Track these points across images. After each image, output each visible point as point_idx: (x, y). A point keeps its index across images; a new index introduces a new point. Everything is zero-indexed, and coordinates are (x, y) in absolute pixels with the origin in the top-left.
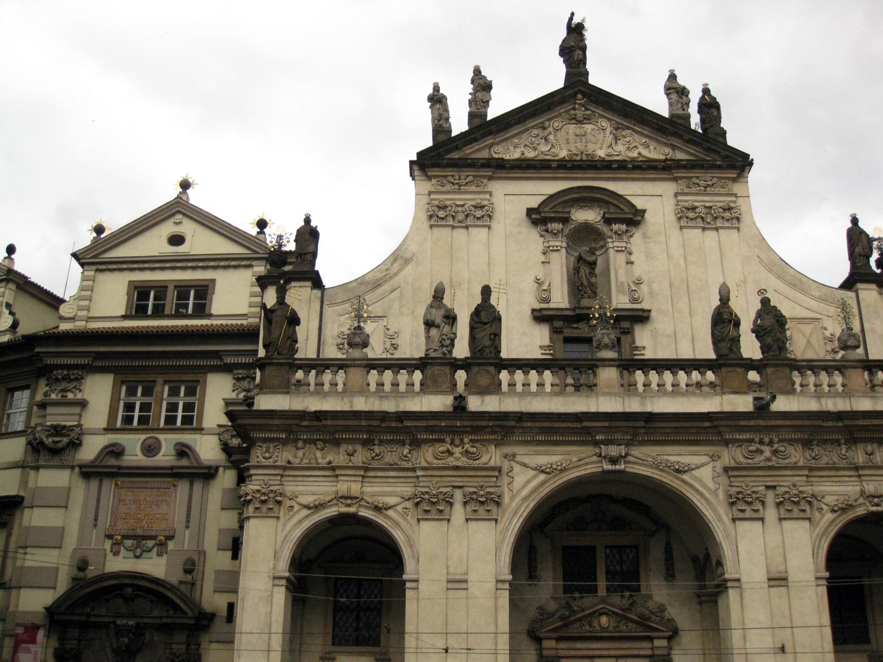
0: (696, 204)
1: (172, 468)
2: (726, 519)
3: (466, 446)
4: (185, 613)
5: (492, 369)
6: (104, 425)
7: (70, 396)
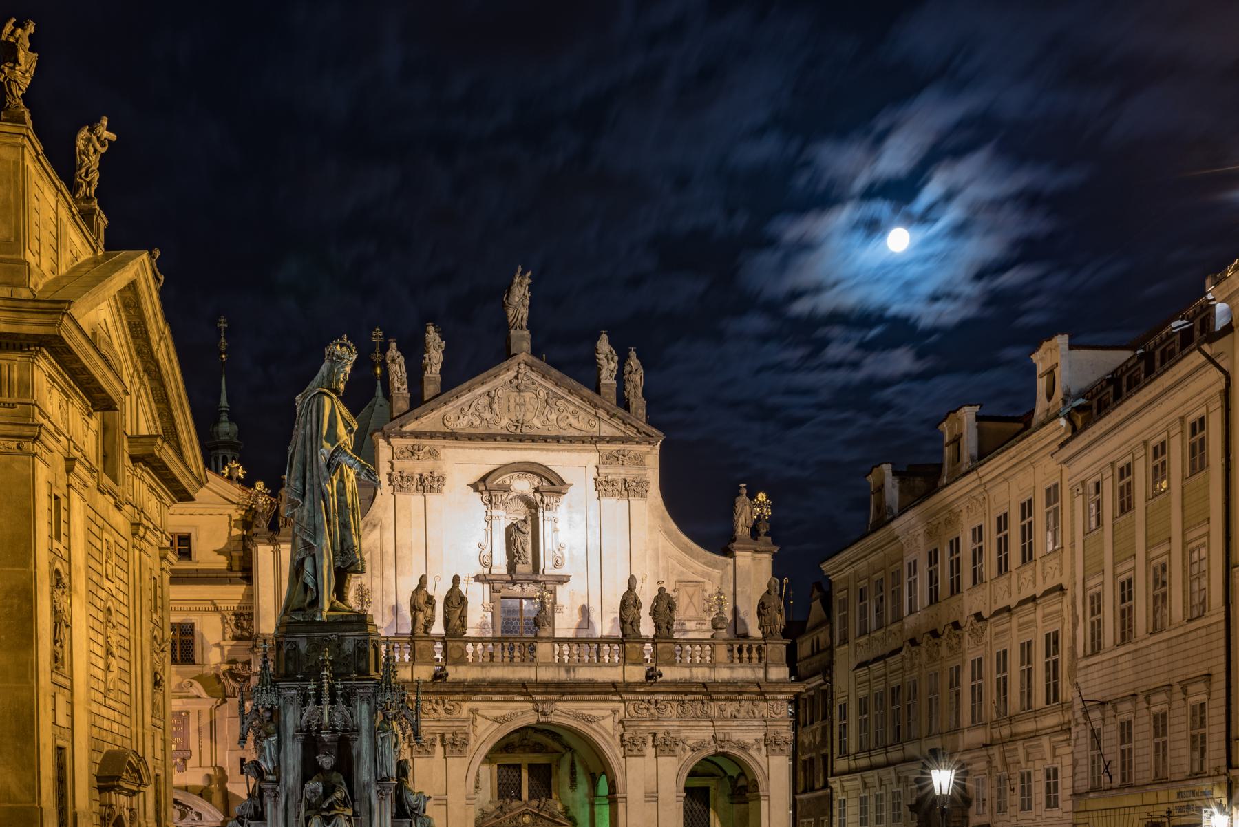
0: (614, 477)
2: (620, 756)
3: (447, 706)
5: (461, 644)
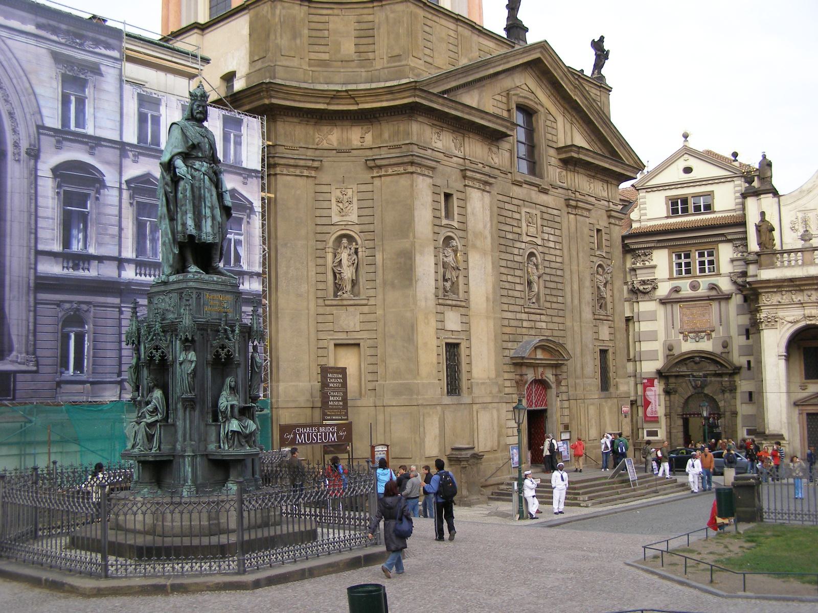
1: (708, 297)
4: (727, 367)
6: (668, 277)
7: (647, 264)
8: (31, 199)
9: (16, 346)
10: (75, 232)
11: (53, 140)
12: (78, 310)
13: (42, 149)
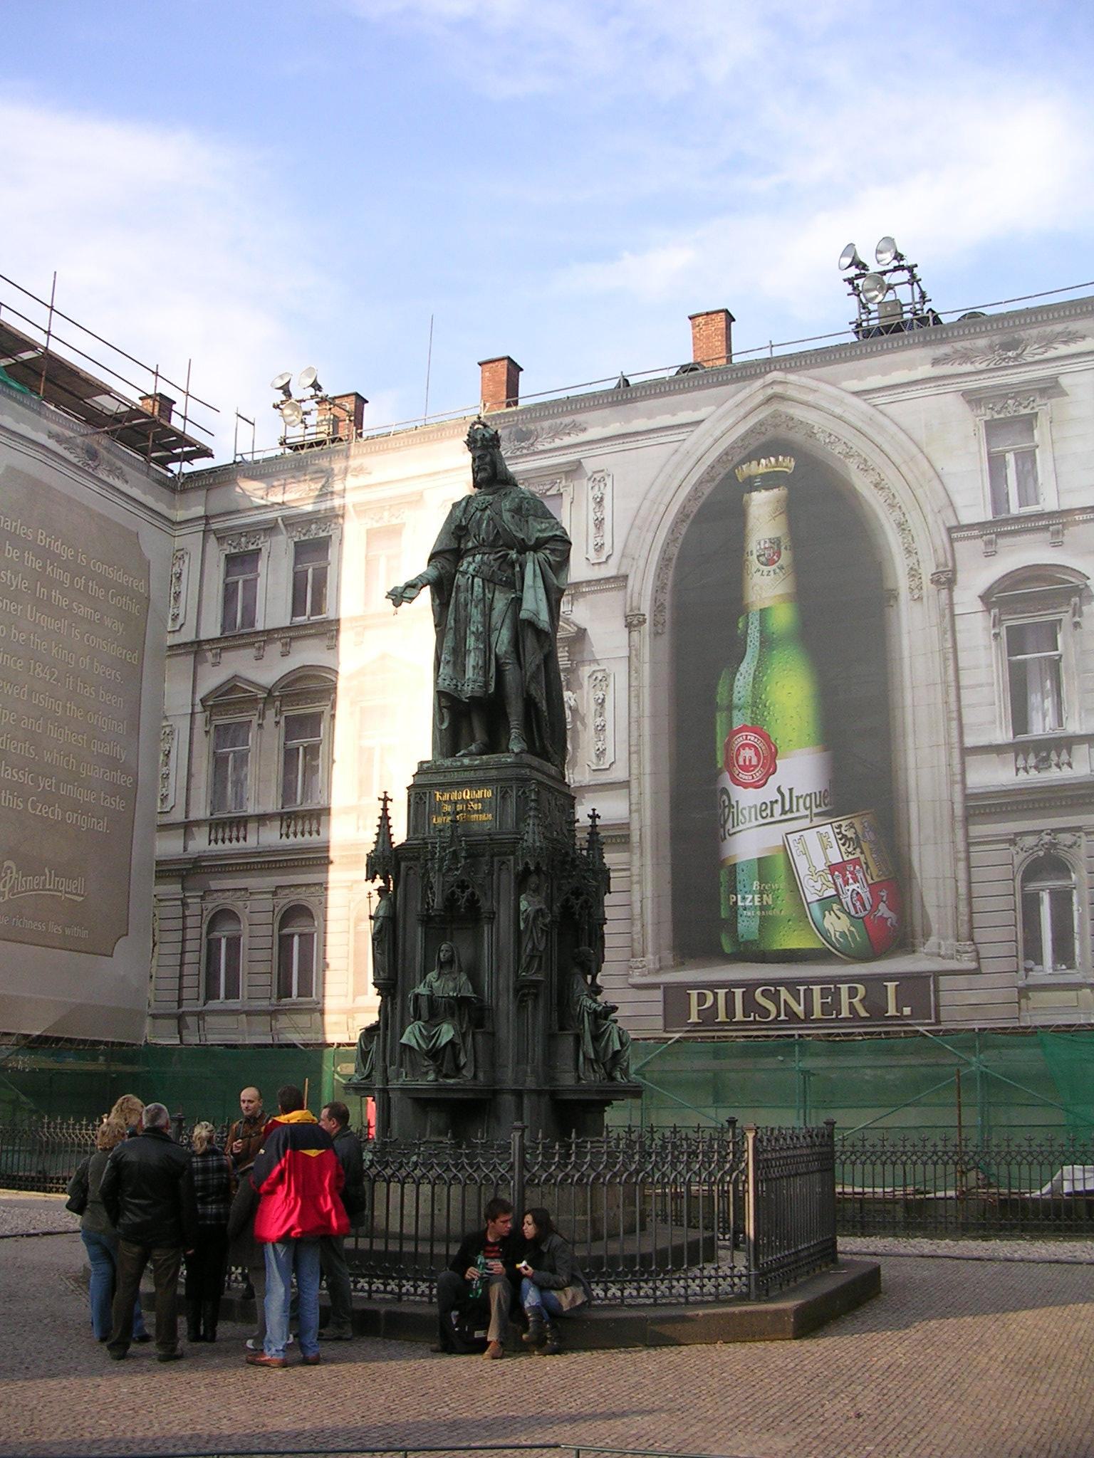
8: (946, 659)
9: (935, 927)
10: (1034, 699)
11: (979, 544)
12: (1053, 845)
13: (959, 568)
